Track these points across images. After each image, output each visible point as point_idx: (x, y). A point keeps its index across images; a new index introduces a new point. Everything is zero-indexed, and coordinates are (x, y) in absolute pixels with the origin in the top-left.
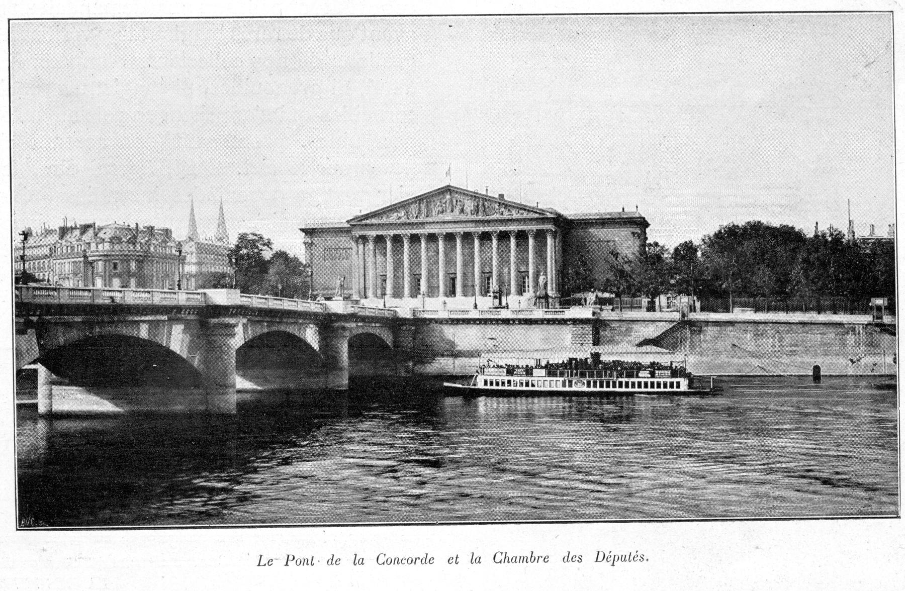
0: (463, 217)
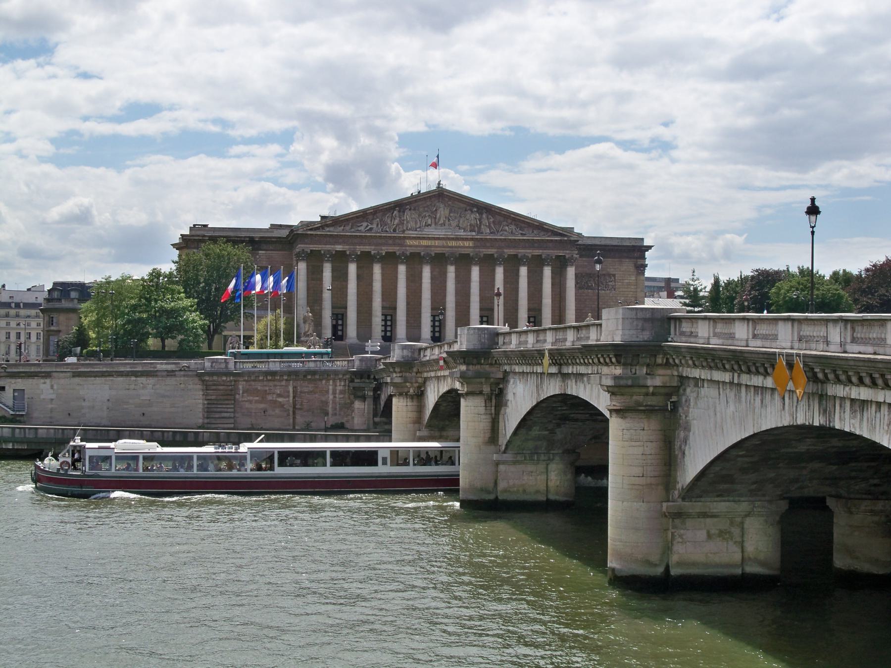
0: (461, 233)
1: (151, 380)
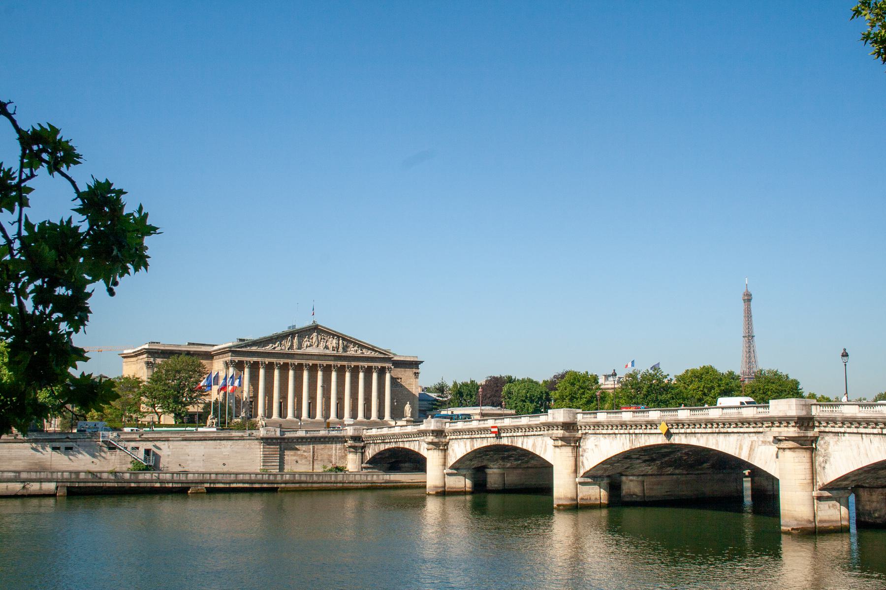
0: (327, 352)
1: (230, 443)
